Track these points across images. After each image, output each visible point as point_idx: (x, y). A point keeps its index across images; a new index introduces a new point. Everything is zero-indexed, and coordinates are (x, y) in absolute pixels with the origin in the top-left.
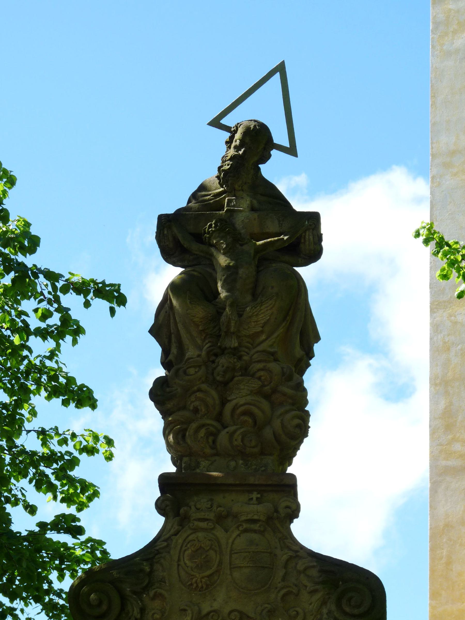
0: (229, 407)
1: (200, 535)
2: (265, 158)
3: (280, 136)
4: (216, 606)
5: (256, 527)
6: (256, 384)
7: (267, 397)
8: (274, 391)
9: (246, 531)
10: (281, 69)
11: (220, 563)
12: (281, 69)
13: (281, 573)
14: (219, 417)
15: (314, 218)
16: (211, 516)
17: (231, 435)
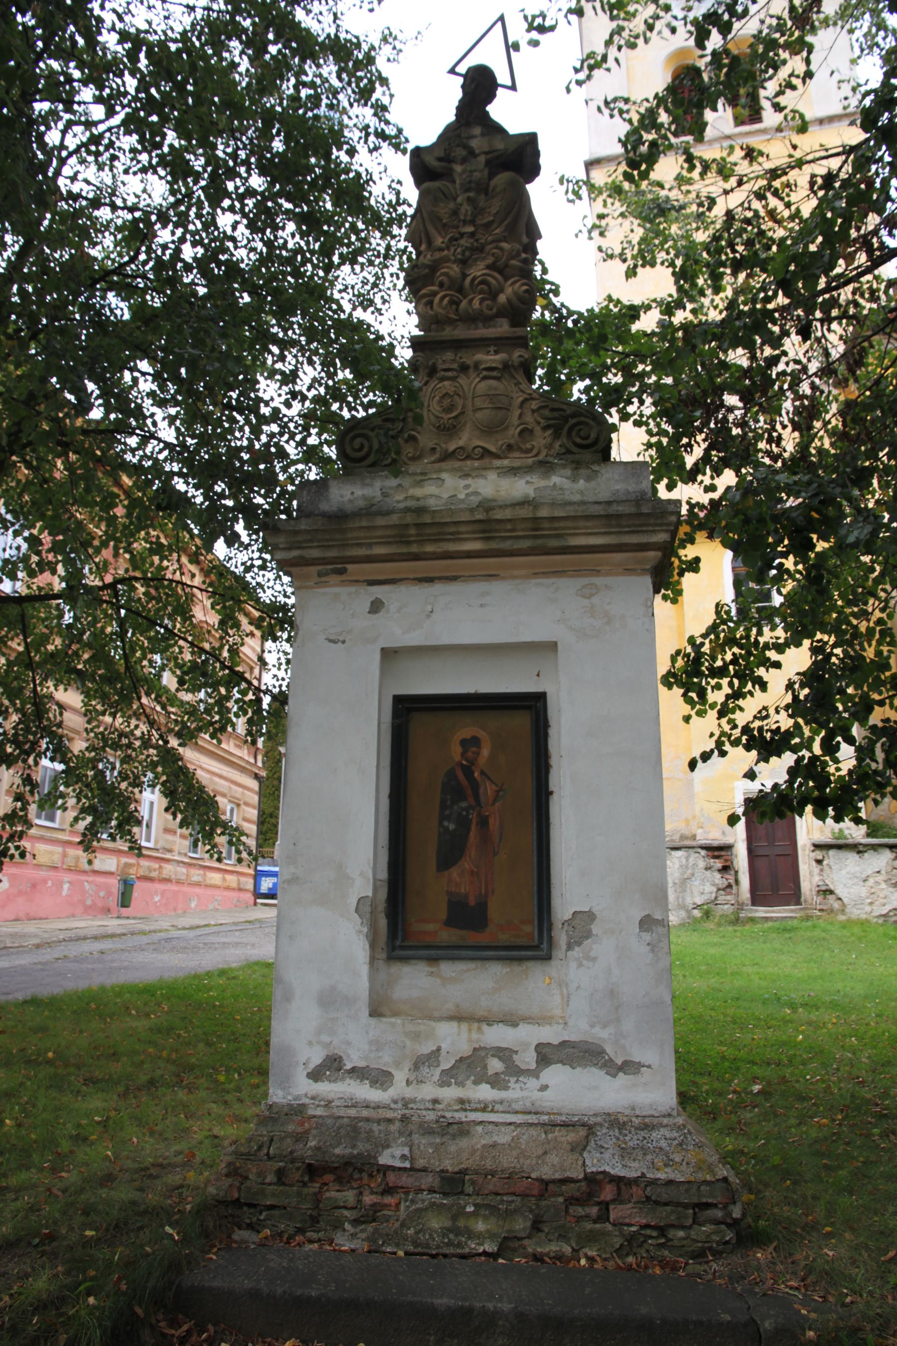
0: (468, 280)
1: (446, 383)
2: (490, 96)
3: (503, 77)
4: (461, 443)
5: (495, 374)
6: (490, 260)
7: (500, 272)
8: (507, 266)
9: (485, 378)
10: (501, 19)
11: (464, 407)
12: (501, 19)
13: (518, 412)
14: (460, 290)
15: (532, 139)
16: (455, 366)
17: (471, 301)
